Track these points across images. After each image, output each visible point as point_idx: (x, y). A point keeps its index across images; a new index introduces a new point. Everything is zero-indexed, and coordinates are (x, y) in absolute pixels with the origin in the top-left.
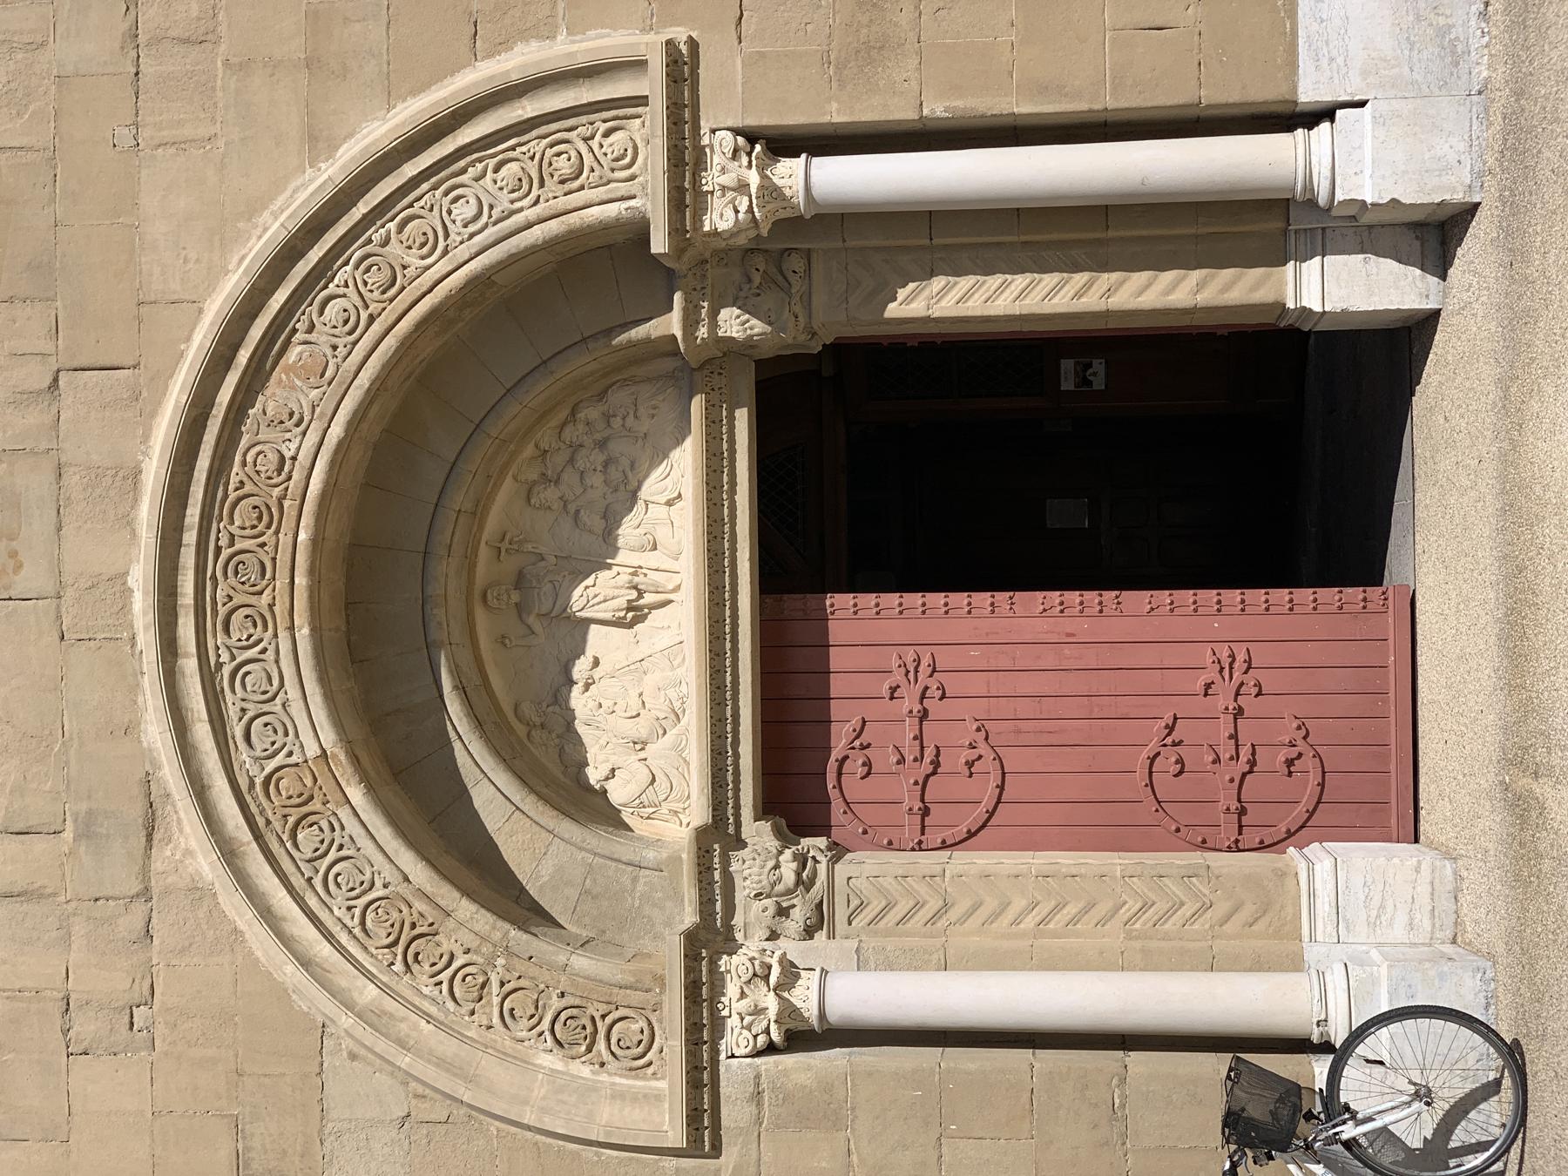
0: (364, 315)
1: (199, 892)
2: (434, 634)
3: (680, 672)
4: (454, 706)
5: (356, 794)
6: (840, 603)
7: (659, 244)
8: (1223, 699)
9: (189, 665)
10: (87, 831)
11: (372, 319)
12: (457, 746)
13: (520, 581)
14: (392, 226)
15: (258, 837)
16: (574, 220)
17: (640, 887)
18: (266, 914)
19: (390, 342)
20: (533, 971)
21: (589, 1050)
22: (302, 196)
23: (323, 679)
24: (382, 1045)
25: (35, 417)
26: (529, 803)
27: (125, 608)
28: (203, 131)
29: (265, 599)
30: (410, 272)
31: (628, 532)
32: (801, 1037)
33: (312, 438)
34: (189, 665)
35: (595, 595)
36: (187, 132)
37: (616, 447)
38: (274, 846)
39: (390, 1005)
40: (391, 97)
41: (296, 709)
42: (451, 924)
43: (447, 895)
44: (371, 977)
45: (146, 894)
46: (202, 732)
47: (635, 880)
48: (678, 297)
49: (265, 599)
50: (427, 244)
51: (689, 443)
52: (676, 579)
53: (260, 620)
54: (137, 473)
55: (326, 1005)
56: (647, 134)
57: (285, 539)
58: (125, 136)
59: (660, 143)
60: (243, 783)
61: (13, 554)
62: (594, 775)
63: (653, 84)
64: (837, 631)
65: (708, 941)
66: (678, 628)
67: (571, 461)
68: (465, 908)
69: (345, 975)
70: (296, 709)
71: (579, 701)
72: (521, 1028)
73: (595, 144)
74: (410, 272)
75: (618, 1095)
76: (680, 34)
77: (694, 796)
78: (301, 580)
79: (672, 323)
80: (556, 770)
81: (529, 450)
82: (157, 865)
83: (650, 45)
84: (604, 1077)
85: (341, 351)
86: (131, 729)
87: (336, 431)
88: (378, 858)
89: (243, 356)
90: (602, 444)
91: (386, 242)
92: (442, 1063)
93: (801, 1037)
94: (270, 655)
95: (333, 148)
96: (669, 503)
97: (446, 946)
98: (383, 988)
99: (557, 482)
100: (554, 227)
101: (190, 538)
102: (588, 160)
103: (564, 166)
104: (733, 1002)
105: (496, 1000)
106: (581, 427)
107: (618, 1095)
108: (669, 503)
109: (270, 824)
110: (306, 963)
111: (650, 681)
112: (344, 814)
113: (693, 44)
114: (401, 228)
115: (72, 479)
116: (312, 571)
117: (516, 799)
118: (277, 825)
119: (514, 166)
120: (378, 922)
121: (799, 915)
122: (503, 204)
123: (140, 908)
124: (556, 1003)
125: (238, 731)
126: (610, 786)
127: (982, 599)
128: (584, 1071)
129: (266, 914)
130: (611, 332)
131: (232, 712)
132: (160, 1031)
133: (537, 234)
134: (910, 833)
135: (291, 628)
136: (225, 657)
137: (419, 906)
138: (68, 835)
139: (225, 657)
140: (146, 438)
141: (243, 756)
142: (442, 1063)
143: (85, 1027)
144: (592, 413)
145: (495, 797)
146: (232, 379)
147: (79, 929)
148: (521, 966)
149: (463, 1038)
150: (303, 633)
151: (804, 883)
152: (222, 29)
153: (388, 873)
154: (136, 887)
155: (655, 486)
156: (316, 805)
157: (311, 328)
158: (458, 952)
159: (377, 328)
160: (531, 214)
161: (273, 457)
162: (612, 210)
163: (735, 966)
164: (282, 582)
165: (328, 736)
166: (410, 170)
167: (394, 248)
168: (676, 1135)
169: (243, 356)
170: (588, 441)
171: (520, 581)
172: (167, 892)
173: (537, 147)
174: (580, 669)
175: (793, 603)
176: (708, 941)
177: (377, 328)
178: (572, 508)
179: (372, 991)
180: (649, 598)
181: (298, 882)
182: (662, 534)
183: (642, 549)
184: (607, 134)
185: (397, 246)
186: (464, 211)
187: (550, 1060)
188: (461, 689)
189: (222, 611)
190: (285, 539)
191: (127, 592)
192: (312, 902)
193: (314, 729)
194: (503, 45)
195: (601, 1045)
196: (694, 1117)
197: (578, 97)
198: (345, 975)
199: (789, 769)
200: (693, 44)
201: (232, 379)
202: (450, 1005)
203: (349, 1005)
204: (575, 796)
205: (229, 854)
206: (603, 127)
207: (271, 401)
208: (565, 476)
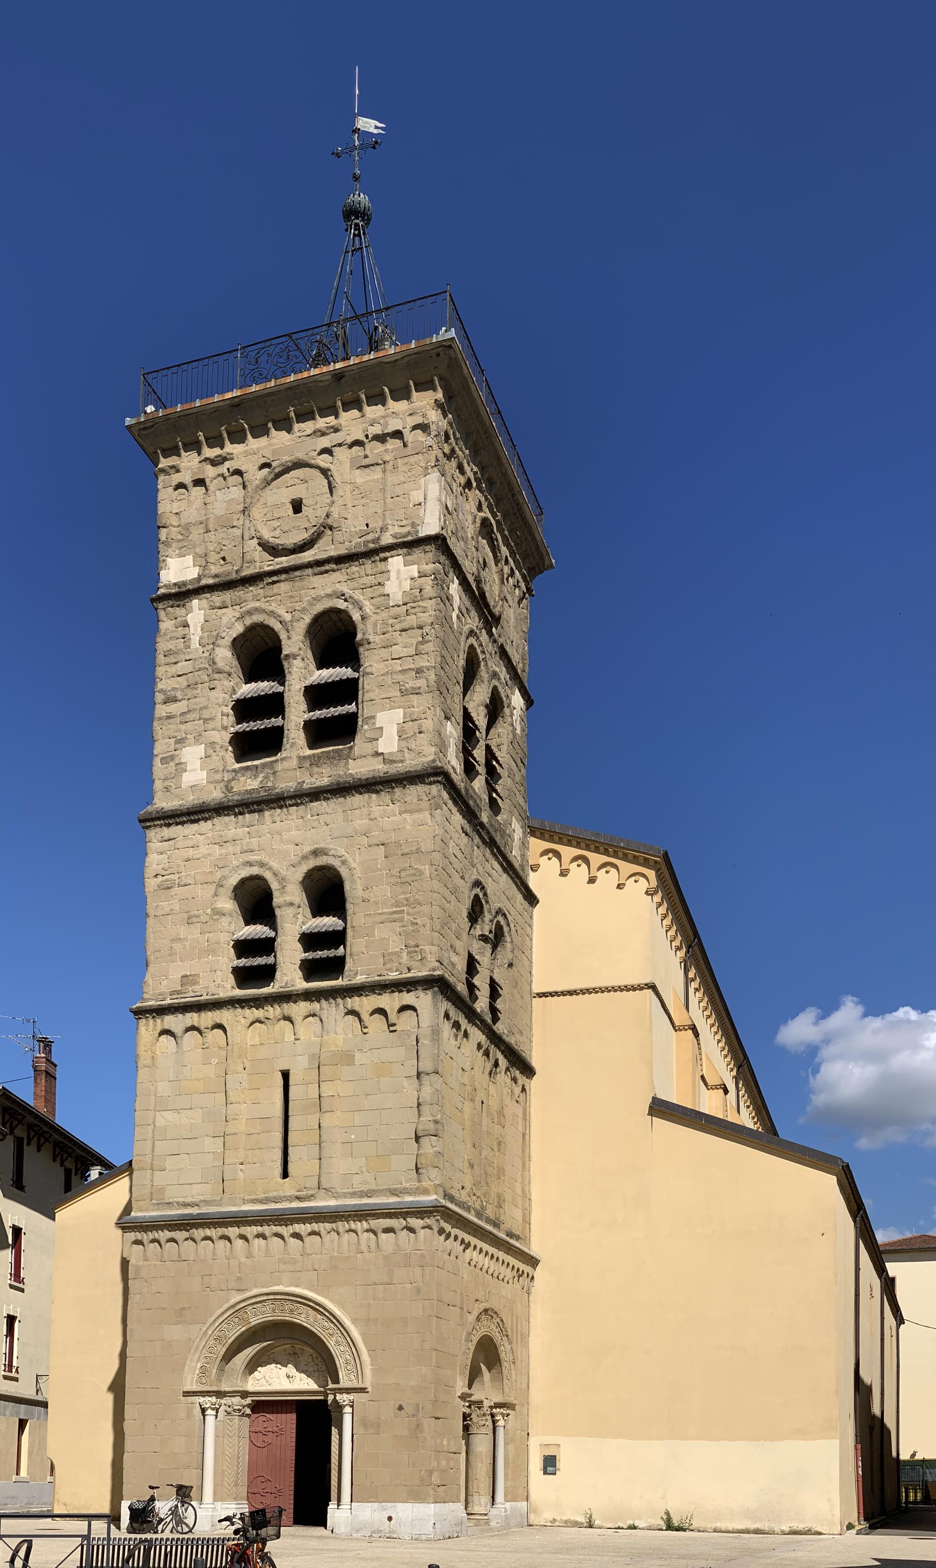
1: (228, 1300)
5: (243, 1329)
6: (294, 1416)
8: (274, 1490)
10: (239, 1278)
13: (295, 1353)
18: (223, 1313)
26: (249, 1358)
31: (303, 1375)
32: (203, 1411)
35: (291, 1369)
43: (227, 1346)
46: (254, 1300)
53: (274, 1310)
55: (208, 1324)
62: (259, 1369)
64: (289, 1415)
65: (220, 1394)
66: (286, 1385)
68: (224, 1349)
69: (213, 1328)
71: (273, 1365)
75: (193, 1378)
86: (256, 1286)
92: (198, 1346)
93: (203, 1411)
104: (207, 1399)
107: (193, 1378)
111: (276, 1379)
121: (229, 1410)
127: (294, 1444)
129: (223, 1313)
130: (329, 1374)
134: (253, 1429)
142: (198, 1346)
143: (206, 1278)
145: (249, 1352)
151: (234, 1410)
155: (310, 1381)
163: (214, 1399)
165: (253, 1323)
171: (295, 1353)
174: (279, 1366)
175: (294, 1406)
176: (220, 1394)
185: (338, 1337)
187: (199, 1365)
193: (254, 1321)
196: (188, 1392)
198: (213, 1328)
199: (263, 1406)
204: (252, 1366)
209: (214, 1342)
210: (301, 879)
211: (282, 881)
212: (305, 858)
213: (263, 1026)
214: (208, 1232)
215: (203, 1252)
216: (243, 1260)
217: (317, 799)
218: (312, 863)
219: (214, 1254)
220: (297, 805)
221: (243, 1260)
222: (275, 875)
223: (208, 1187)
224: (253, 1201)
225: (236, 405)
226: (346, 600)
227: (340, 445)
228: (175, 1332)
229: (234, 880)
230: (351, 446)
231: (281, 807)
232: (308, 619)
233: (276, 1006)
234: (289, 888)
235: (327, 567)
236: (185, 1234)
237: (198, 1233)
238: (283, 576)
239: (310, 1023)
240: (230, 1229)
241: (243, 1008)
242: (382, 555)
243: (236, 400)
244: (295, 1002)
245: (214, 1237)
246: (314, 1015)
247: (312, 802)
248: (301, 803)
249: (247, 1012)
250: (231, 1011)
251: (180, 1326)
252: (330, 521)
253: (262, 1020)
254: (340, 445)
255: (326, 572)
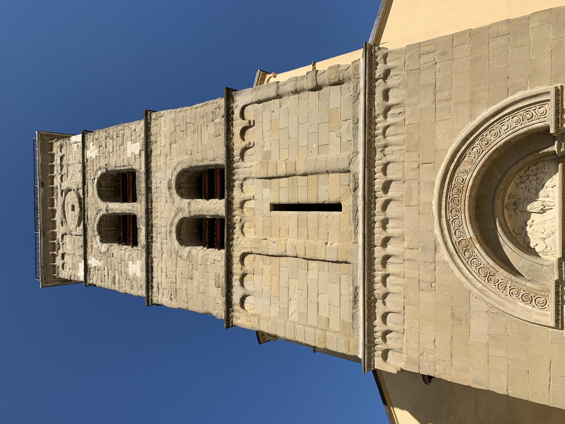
0: (481, 150)
1: (445, 263)
2: (495, 215)
3: (554, 224)
4: (499, 229)
5: (478, 246)
7: (552, 131)
9: (444, 219)
10: (423, 250)
11: (483, 151)
12: (500, 237)
14: (488, 132)
15: (457, 253)
16: (531, 127)
17: (543, 270)
18: (459, 268)
19: (487, 155)
20: (517, 285)
21: (531, 303)
22: (469, 128)
23: (471, 223)
24: (483, 296)
25: (415, 173)
26: (517, 250)
27: (431, 208)
28: (449, 117)
29: (459, 207)
30: (492, 141)
31: (541, 193)
33: (470, 175)
34: (444, 219)
36: (446, 117)
37: (539, 175)
38: (460, 255)
39: (484, 288)
40: (488, 106)
41: (465, 228)
42: (498, 273)
43: (497, 268)
44: (480, 282)
45: (435, 262)
46: (446, 232)
47: (542, 268)
48: (556, 142)
49: (459, 207)
50: (496, 135)
51: (558, 174)
52: (554, 204)
54: (434, 183)
55: (472, 287)
56: (550, 108)
57: (463, 195)
58: (433, 119)
59: (553, 109)
60: (454, 243)
61: (410, 198)
62: (532, 245)
63: (552, 97)
67: (528, 178)
68: (502, 271)
69: (475, 281)
70: (465, 228)
71: (528, 229)
72: (514, 297)
73: (536, 111)
74: (492, 141)
76: (559, 85)
77: (557, 251)
78: (467, 203)
79: (555, 148)
80: (523, 244)
81: (518, 176)
82: (437, 257)
83: (551, 89)
84: (534, 309)
85: (476, 158)
86: (432, 231)
87: (475, 174)
88: (482, 259)
89: (456, 160)
90: (536, 175)
91: (486, 136)
92: (496, 301)
94: (460, 218)
95: (475, 118)
96: (552, 187)
97: (497, 278)
98: (483, 285)
99: (524, 183)
100: (526, 129)
101: (444, 195)
102: (534, 114)
103: (528, 116)
105: (508, 290)
106: (530, 171)
108: (552, 187)
109: (459, 250)
110: (467, 278)
111: (546, 226)
112: (475, 250)
113: (562, 87)
114: (490, 132)
115: (422, 184)
116: (469, 201)
117: (513, 249)
118: (461, 251)
119: (516, 117)
120: (482, 271)
122: (514, 125)
123: (433, 265)
124: (523, 293)
125: (453, 232)
126: (536, 248)
128: (530, 307)
129: (459, 268)
131: (452, 229)
132: (437, 288)
133: (522, 131)
135: (464, 212)
136: (451, 218)
137: (491, 269)
138: (420, 250)
139: (451, 218)
140: (436, 176)
141: (454, 237)
142: (496, 301)
143: (423, 286)
144: (533, 168)
145: (508, 248)
146: (453, 164)
147: (422, 267)
148: (514, 284)
149: (501, 297)
150: (467, 214)
152: (453, 97)
153: (484, 262)
154: (433, 260)
155: (548, 183)
156: (469, 247)
157: (470, 154)
158: (500, 279)
159: (484, 153)
160: (520, 127)
161: (461, 179)
162: (540, 124)
164: (463, 203)
165: (472, 234)
166: (492, 120)
167: (488, 136)
168: (552, 324)
169: (456, 160)
170: (532, 174)
171: (515, 204)
172: (439, 262)
173: (522, 113)
174: (529, 222)
177: (484, 153)
178: (528, 188)
179: (480, 285)
180: (546, 208)
181: (465, 262)
182: (550, 194)
183: (545, 197)
184: (539, 108)
185: (489, 136)
186: (504, 128)
187: (522, 304)
188: (501, 225)
189: (450, 209)
190: (463, 195)
191: (432, 205)
192: (468, 266)
193: (469, 232)
194: (515, 92)
195: (533, 302)
196: (557, 321)
197: (536, 100)
198: (475, 281)
200: (562, 87)
201: (453, 164)
202: (498, 290)
203: (476, 288)
205: (451, 256)
206: (538, 107)
207: (461, 168)
208: (526, 182)
209: (492, 283)
210: (180, 198)
211: (179, 210)
212: (171, 194)
213: (245, 225)
214: (378, 279)
215: (398, 287)
216: (406, 244)
217: (151, 189)
218: (174, 191)
219: (398, 276)
220: (152, 202)
221: (406, 244)
222: (176, 215)
223: (344, 278)
224: (356, 233)
225: (44, 233)
226: (94, 179)
227: (61, 186)
228: (479, 327)
229: (176, 243)
230: (62, 181)
231: (152, 212)
232: (99, 200)
233: (234, 213)
234: (182, 206)
235: (86, 190)
236: (379, 303)
237: (379, 289)
238: (86, 213)
239: (246, 188)
240: (376, 255)
241: (233, 239)
242: (85, 161)
243: (42, 233)
244: (233, 198)
245: (382, 273)
246: (242, 185)
247: (151, 193)
248: (151, 199)
249: (235, 236)
250: (234, 249)
251: (472, 322)
252: (76, 189)
253: (241, 225)
254: (61, 186)
255: (87, 190)
